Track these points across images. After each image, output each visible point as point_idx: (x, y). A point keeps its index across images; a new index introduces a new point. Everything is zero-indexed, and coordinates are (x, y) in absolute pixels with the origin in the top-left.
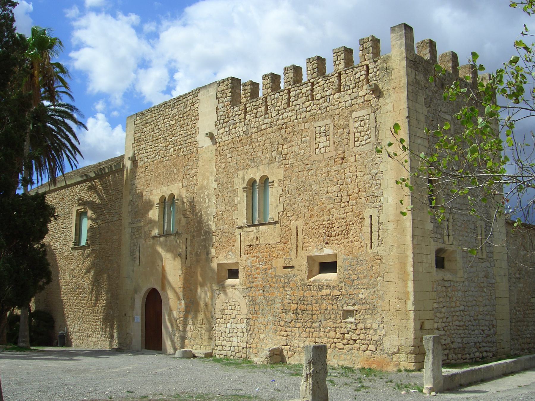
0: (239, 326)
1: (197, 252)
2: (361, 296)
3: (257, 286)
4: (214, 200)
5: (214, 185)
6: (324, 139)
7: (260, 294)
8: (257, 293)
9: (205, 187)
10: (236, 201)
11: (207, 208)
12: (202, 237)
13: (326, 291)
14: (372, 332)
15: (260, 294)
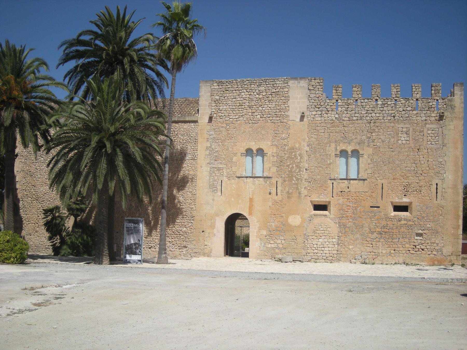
0: (331, 240)
1: (288, 192)
2: (428, 226)
3: (347, 216)
4: (306, 158)
5: (307, 149)
6: (405, 135)
7: (350, 222)
8: (347, 221)
9: (296, 148)
10: (329, 162)
11: (299, 163)
12: (293, 182)
13: (403, 222)
14: (435, 245)
15: (350, 222)
